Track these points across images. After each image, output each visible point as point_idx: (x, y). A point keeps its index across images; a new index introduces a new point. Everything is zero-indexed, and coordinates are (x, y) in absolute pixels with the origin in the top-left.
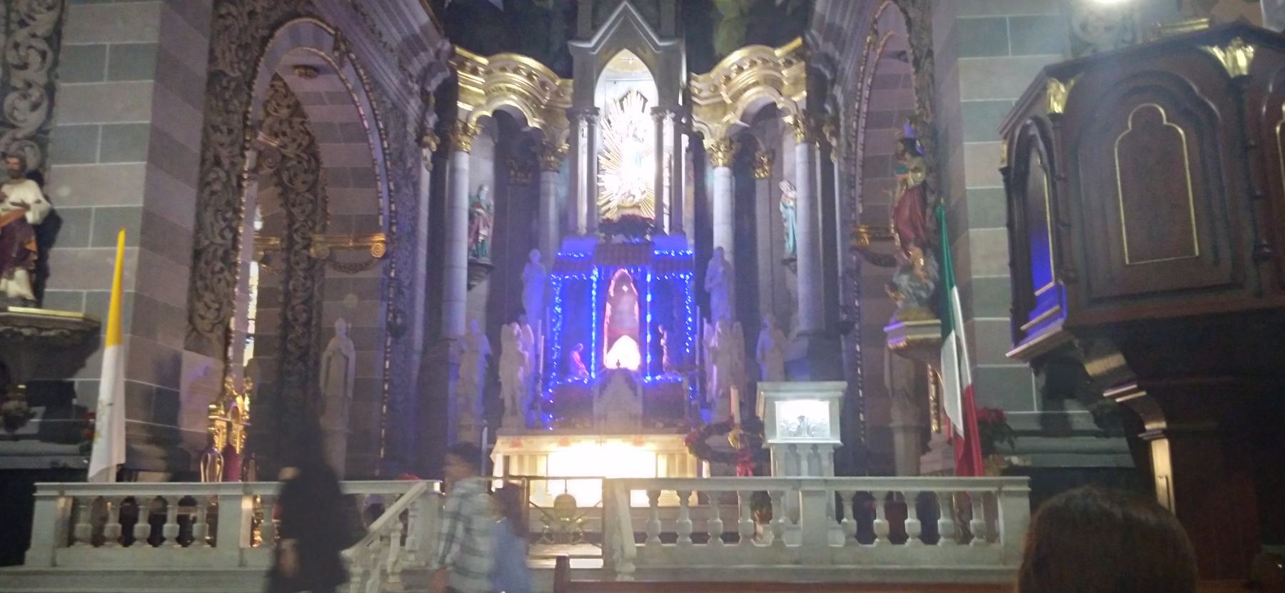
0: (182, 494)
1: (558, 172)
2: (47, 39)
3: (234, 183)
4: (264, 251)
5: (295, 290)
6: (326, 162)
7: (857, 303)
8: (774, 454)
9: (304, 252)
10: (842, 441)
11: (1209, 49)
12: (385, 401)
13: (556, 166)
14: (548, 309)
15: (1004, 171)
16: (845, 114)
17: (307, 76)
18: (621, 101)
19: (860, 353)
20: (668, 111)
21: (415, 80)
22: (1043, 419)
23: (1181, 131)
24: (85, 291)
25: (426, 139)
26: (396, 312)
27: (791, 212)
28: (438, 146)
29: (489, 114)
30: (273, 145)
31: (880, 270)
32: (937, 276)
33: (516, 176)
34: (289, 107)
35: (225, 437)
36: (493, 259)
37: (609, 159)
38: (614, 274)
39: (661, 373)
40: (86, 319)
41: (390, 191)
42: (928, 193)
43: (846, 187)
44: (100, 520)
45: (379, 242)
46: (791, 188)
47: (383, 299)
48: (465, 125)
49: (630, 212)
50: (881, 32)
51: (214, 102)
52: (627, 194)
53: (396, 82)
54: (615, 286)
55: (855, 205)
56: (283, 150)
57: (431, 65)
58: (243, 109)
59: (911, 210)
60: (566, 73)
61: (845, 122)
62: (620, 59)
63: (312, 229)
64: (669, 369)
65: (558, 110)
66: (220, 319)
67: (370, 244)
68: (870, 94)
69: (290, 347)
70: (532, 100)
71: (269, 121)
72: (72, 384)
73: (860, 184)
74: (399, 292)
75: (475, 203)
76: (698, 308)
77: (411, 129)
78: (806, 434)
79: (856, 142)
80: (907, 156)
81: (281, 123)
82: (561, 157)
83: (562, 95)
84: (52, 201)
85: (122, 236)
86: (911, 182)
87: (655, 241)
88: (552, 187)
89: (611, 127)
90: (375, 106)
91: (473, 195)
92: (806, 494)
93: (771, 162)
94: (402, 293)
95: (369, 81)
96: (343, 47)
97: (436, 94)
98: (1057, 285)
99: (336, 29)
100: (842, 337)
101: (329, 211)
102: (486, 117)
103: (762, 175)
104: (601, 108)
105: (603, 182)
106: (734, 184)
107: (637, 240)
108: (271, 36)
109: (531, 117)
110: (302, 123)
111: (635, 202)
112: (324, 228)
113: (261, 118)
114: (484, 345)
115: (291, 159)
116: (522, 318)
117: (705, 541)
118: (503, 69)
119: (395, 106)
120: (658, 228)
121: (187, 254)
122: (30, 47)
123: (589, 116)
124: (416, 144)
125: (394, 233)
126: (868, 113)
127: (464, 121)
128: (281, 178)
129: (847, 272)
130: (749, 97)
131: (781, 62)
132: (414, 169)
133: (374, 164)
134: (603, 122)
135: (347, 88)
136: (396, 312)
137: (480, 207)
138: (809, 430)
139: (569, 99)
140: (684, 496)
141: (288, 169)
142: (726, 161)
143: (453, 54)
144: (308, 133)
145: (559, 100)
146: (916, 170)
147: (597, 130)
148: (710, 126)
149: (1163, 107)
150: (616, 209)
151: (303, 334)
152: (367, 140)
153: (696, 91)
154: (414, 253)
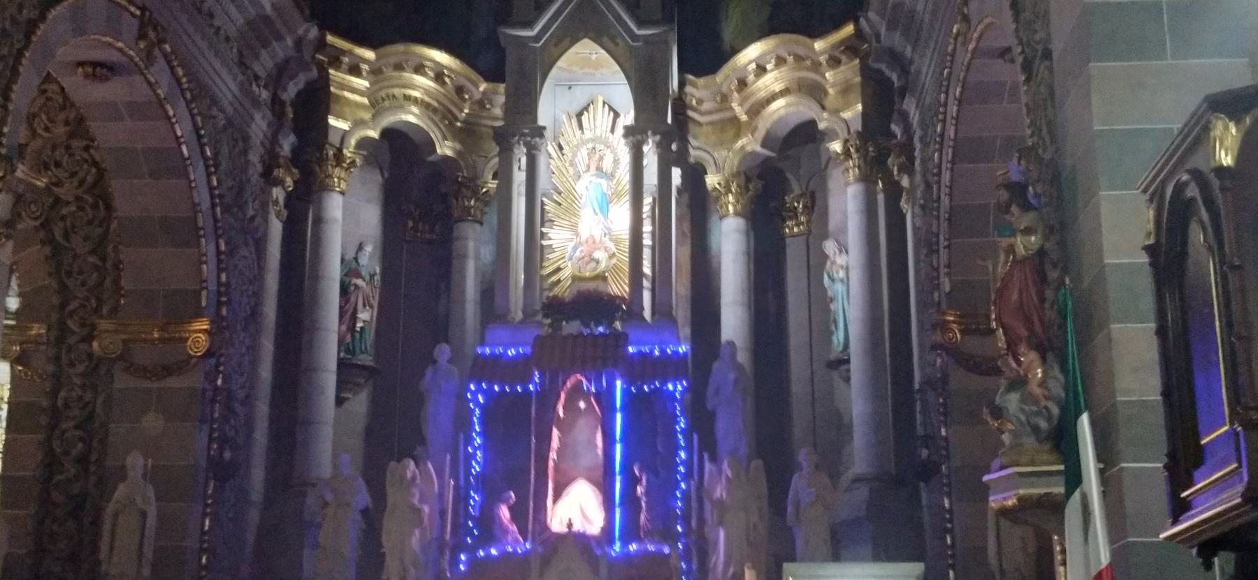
1: (481, 223)
4: (21, 344)
5: (67, 406)
6: (124, 207)
7: (943, 432)
13: (479, 215)
14: (462, 436)
16: (921, 139)
17: (94, 77)
18: (579, 115)
19: (950, 511)
20: (649, 133)
21: (263, 84)
25: (279, 173)
26: (224, 442)
27: (839, 287)
28: (295, 182)
29: (374, 134)
30: (39, 183)
31: (976, 382)
32: (1063, 395)
33: (415, 229)
36: (377, 356)
37: (560, 204)
38: (564, 383)
39: (638, 539)
41: (219, 252)
42: (1048, 267)
45: (200, 331)
46: (840, 251)
47: (202, 421)
48: (340, 150)
49: (591, 286)
50: (974, 22)
54: (566, 401)
55: (938, 278)
57: (287, 61)
59: (1020, 294)
60: (494, 75)
61: (922, 151)
62: (577, 53)
63: (97, 311)
64: (650, 534)
65: (484, 130)
67: (187, 335)
68: (958, 111)
69: (57, 496)
70: (441, 112)
71: (38, 143)
73: (945, 247)
74: (229, 410)
75: (351, 270)
76: (695, 436)
77: (254, 157)
79: (939, 182)
80: (1014, 209)
81: (54, 148)
82: (485, 200)
83: (488, 106)
86: (1021, 251)
87: (628, 332)
88: (471, 245)
89: (563, 155)
90: (200, 125)
91: (347, 258)
93: (809, 209)
94: (233, 412)
95: (192, 85)
101: (123, 283)
102: (372, 139)
103: (796, 230)
105: (550, 239)
106: (752, 243)
107: (601, 329)
108: (43, 18)
111: (598, 271)
112: (114, 311)
113: (23, 141)
114: (363, 497)
115: (68, 203)
116: (419, 450)
118: (399, 67)
119: (230, 123)
120: (632, 310)
123: (529, 139)
125: (223, 318)
126: (955, 140)
127: (338, 146)
129: (927, 382)
131: (823, 59)
132: (258, 220)
133: (196, 212)
134: (551, 148)
135: (157, 95)
136: (224, 442)
137: (359, 276)
139: (498, 111)
141: (63, 218)
142: (739, 207)
143: (321, 45)
144: (95, 164)
145: (484, 114)
146: (1028, 231)
147: (542, 161)
148: (716, 155)
154: (254, 348)
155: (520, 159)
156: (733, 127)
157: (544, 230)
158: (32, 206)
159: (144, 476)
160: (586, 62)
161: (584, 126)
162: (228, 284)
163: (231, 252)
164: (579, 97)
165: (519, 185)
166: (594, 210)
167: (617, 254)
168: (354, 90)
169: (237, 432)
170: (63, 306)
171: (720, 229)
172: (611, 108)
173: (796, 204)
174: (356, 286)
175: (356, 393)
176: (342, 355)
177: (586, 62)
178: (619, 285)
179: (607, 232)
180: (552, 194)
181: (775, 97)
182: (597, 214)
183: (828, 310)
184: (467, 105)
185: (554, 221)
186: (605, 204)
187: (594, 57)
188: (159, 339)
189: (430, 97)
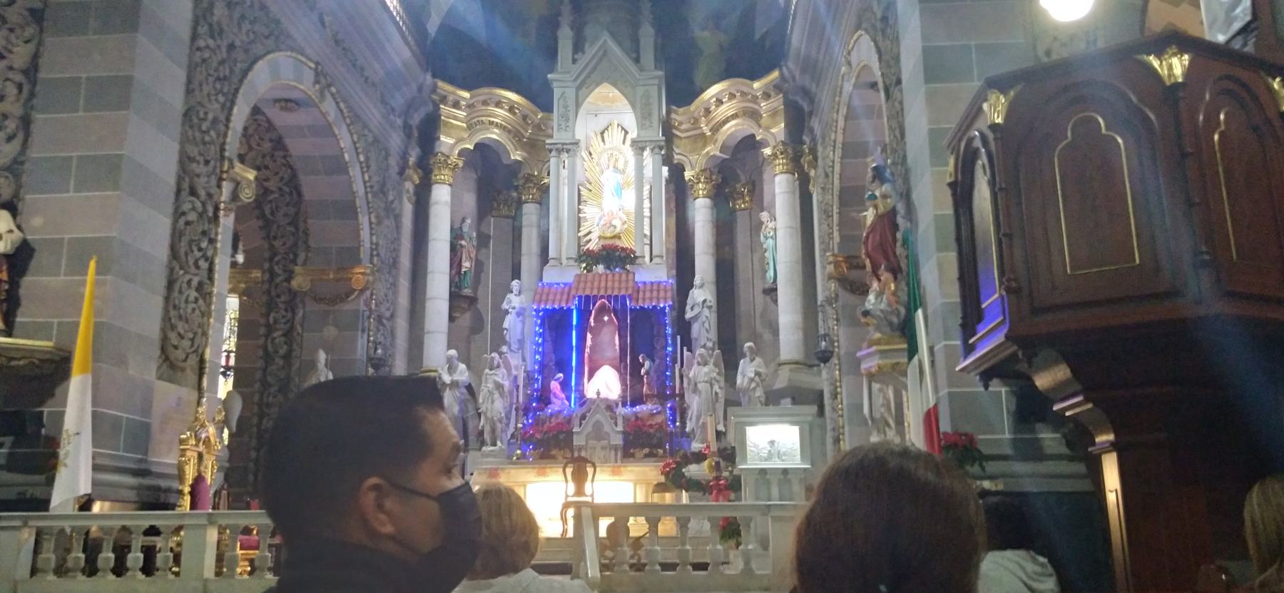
0: (146, 524)
2: (25, 72)
3: (211, 214)
4: (245, 283)
5: (276, 322)
6: (307, 194)
8: (745, 480)
9: (285, 284)
10: (812, 465)
11: (1139, 57)
15: (952, 185)
18: (602, 133)
21: (397, 114)
22: (1015, 442)
23: (1120, 141)
24: (56, 321)
25: (410, 172)
27: (770, 242)
29: (471, 147)
34: (271, 140)
35: (196, 467)
37: (590, 191)
38: (594, 305)
40: (53, 347)
41: (371, 223)
43: (824, 217)
44: (64, 549)
51: (190, 133)
52: (608, 225)
53: (377, 114)
54: (595, 316)
55: (832, 233)
56: (265, 184)
58: (221, 140)
63: (294, 262)
66: (193, 349)
67: (351, 276)
71: (252, 154)
72: (42, 412)
76: (679, 337)
77: (393, 162)
78: (777, 459)
79: (833, 172)
81: (264, 156)
84: (25, 231)
85: (92, 264)
91: (455, 227)
92: (775, 519)
93: (751, 192)
94: (383, 325)
95: (351, 114)
96: (323, 81)
97: (418, 128)
98: (1002, 297)
99: (317, 63)
100: (822, 365)
103: (743, 206)
109: (512, 147)
110: (285, 157)
115: (272, 192)
117: (674, 570)
118: (485, 103)
119: (376, 140)
121: (161, 283)
122: (7, 79)
124: (398, 177)
128: (263, 211)
130: (728, 129)
132: (396, 202)
134: (584, 154)
137: (462, 238)
138: (779, 455)
140: (653, 524)
141: (270, 202)
143: (434, 89)
144: (291, 167)
149: (1102, 116)
151: (283, 368)
152: (348, 173)
154: (394, 285)
156: (702, 139)
159: (326, 366)
162: (377, 244)
163: (379, 223)
168: (456, 118)
169: (385, 338)
170: (271, 259)
172: (623, 128)
174: (461, 245)
175: (462, 313)
176: (453, 289)
183: (763, 258)
184: (530, 128)
186: (620, 189)
187: (611, 95)
188: (333, 279)
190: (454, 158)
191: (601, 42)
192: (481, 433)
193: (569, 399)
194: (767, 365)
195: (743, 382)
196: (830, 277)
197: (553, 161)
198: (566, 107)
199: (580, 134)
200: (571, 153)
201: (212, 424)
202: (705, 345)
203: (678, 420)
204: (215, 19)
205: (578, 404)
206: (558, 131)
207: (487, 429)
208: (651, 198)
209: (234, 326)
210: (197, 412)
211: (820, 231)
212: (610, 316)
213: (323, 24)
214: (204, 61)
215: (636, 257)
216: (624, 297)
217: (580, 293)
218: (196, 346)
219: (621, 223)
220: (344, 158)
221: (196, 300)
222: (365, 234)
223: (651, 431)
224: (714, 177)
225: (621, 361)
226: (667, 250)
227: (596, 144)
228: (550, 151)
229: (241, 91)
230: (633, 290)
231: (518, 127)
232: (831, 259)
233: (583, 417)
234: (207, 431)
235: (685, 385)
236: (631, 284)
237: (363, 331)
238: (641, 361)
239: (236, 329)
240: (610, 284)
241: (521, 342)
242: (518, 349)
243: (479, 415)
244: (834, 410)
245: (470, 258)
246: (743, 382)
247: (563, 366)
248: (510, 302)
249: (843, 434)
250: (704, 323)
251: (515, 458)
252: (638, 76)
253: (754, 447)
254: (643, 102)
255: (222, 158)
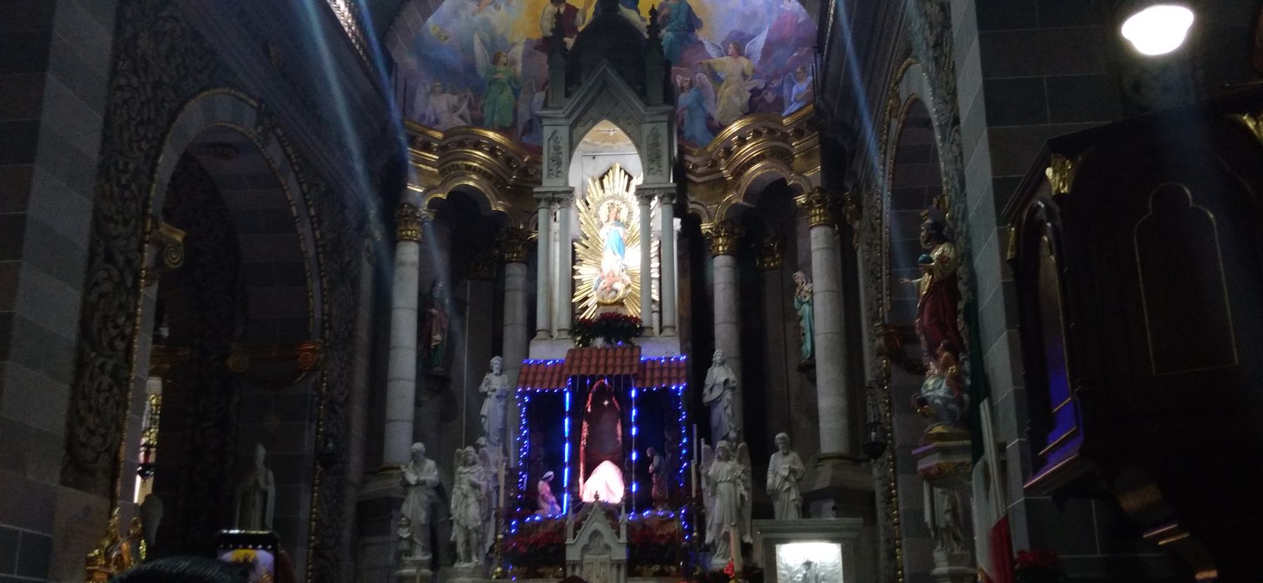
12: (312, 545)
18: (601, 179)
27: (806, 308)
29: (442, 196)
37: (588, 248)
38: (592, 385)
41: (322, 290)
49: (612, 309)
55: (882, 299)
62: (599, 131)
64: (661, 501)
79: (881, 225)
99: (260, 101)
100: (873, 461)
104: (576, 189)
105: (580, 274)
111: (617, 298)
118: (461, 144)
134: (580, 204)
137: (432, 306)
150: (596, 306)
153: (691, 167)
155: (555, 214)
156: (722, 185)
157: (575, 267)
158: (173, 254)
160: (606, 138)
161: (605, 187)
162: (330, 315)
164: (602, 164)
165: (555, 233)
166: (614, 252)
167: (632, 285)
168: (426, 162)
171: (713, 262)
172: (626, 173)
173: (772, 244)
174: (431, 314)
177: (606, 138)
178: (634, 310)
179: (624, 268)
180: (581, 240)
181: (754, 162)
182: (615, 254)
183: (798, 327)
185: (582, 261)
186: (622, 246)
187: (612, 133)
189: (488, 168)
190: (423, 210)
191: (601, 70)
192: (453, 546)
193: (560, 503)
194: (804, 459)
195: (774, 481)
196: (880, 353)
197: (542, 214)
198: (557, 148)
199: (574, 181)
200: (564, 203)
201: (125, 538)
202: (728, 434)
203: (695, 529)
204: (138, 51)
205: (571, 510)
206: (548, 177)
207: (460, 540)
208: (659, 256)
209: (156, 414)
210: (109, 524)
211: (867, 295)
212: (610, 400)
213: (267, 52)
214: (125, 102)
215: (642, 329)
216: (627, 377)
217: (574, 372)
218: (109, 442)
219: (624, 286)
220: (290, 211)
221: (110, 387)
222: (315, 302)
223: (662, 542)
224: (737, 230)
225: (624, 457)
226: (681, 318)
227: (594, 191)
228: (539, 201)
229: (169, 136)
230: (639, 369)
231: (500, 173)
232: (880, 330)
233: (578, 526)
234: (120, 548)
235: (704, 485)
236: (635, 361)
237: (311, 421)
238: (649, 455)
239: (157, 417)
240: (610, 361)
241: (504, 431)
242: (499, 441)
243: (452, 522)
244: (889, 517)
245: (442, 329)
246: (774, 481)
247: (555, 462)
248: (489, 383)
249: (900, 547)
250: (726, 408)
251: (494, 577)
252: (642, 111)
253: (786, 569)
254: (651, 142)
255: (145, 214)
